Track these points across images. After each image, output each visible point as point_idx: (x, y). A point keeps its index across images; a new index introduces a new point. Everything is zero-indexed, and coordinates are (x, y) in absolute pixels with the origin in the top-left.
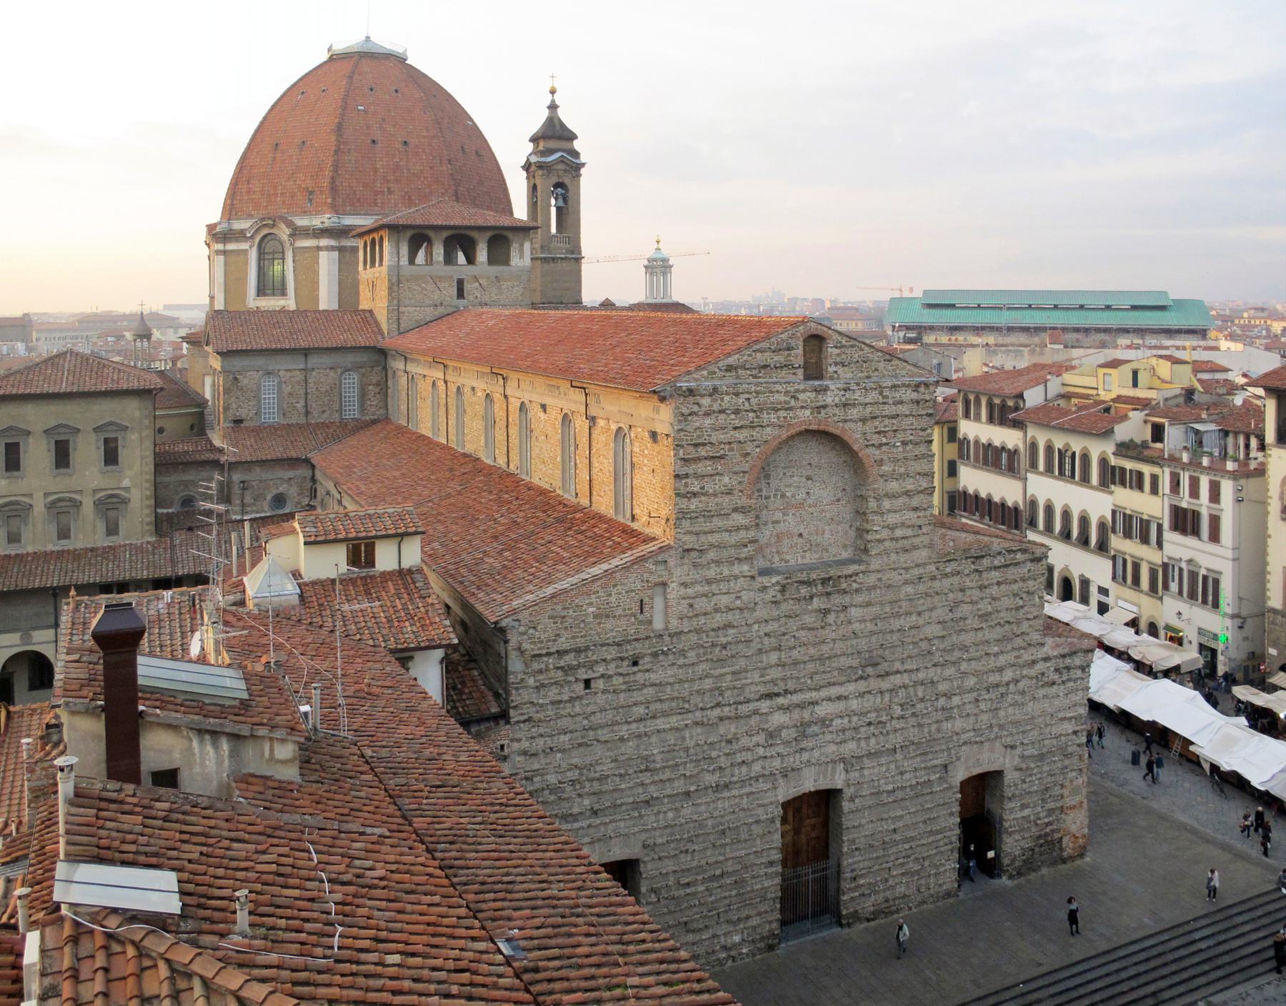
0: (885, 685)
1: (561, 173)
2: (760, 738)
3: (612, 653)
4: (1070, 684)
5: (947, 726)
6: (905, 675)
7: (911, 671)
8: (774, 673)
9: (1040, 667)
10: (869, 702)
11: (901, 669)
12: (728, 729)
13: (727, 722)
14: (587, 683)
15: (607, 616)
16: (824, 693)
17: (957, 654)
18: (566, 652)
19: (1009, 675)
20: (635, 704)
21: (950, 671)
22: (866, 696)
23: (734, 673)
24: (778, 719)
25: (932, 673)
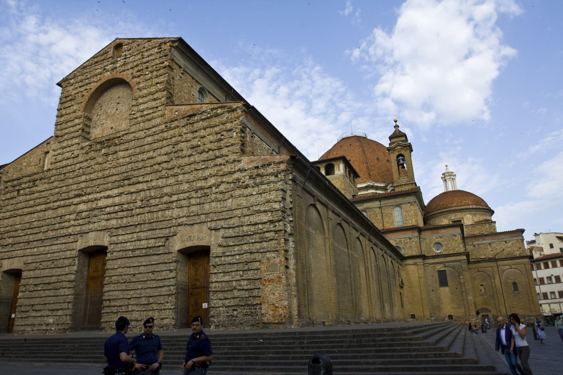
0: (133, 189)
1: (399, 150)
2: (73, 217)
3: (28, 179)
4: (264, 187)
5: (168, 213)
6: (145, 184)
7: (148, 181)
8: (82, 185)
9: (236, 175)
10: (124, 199)
11: (142, 181)
12: (61, 211)
13: (61, 208)
14: (19, 191)
15: (29, 166)
16: (102, 194)
17: (176, 170)
18: (14, 180)
19: (212, 181)
20: (31, 200)
21: (171, 181)
22: (123, 196)
23: (66, 186)
24: (82, 207)
25: (160, 183)
